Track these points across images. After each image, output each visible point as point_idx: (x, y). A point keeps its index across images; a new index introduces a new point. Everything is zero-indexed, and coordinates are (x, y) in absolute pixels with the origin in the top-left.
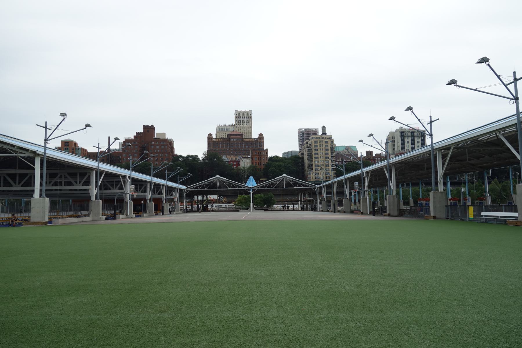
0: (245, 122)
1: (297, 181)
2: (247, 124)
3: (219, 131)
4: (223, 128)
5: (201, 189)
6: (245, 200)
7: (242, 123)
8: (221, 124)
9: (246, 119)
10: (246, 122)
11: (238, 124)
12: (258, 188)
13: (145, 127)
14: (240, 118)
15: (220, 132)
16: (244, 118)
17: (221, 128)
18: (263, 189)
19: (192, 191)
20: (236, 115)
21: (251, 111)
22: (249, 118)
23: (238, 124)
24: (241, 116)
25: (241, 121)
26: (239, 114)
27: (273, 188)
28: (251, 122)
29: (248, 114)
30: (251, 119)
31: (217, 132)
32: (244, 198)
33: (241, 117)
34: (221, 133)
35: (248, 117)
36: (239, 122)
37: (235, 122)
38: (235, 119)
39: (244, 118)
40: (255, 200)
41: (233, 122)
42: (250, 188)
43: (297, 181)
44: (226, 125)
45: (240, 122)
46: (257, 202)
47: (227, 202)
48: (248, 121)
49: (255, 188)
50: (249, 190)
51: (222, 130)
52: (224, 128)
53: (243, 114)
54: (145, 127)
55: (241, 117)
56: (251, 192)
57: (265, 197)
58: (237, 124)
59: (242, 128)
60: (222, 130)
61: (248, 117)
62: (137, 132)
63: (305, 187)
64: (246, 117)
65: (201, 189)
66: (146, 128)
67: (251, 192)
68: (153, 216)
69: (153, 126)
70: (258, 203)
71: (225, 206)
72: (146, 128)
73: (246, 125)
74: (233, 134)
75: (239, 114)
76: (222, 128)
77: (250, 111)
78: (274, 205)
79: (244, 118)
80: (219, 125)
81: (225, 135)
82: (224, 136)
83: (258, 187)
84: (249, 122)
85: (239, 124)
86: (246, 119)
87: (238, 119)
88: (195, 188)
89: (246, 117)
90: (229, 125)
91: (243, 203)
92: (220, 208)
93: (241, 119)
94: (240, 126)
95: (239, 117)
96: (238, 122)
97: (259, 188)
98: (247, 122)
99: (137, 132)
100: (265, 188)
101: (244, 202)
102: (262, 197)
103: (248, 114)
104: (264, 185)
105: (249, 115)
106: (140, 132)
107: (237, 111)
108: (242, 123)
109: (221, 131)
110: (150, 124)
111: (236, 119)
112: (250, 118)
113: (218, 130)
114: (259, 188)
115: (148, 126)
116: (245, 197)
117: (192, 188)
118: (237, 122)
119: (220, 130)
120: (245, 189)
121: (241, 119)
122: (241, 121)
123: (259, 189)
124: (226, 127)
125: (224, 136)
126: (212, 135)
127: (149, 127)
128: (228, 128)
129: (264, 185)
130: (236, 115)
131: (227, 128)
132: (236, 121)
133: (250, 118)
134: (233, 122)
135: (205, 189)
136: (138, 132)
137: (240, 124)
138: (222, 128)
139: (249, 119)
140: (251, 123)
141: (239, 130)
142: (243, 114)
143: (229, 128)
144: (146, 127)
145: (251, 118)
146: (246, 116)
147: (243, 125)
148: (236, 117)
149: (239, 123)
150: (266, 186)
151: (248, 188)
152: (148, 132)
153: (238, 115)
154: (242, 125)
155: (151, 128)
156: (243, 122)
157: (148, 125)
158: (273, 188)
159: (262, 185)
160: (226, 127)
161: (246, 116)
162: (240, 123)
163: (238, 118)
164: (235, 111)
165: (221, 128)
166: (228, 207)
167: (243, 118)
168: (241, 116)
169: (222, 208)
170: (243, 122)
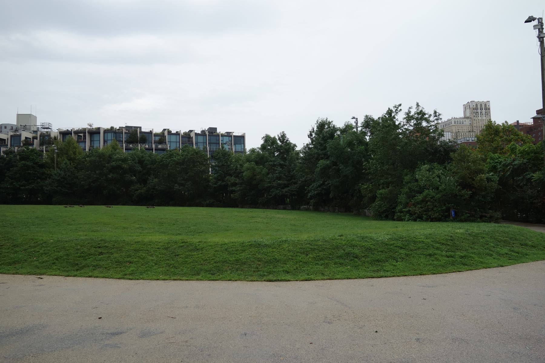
0: (483, 115)
3: (455, 124)
7: (479, 115)
9: (484, 111)
11: (476, 117)
14: (478, 109)
15: (456, 125)
16: (482, 109)
17: (456, 120)
20: (474, 106)
22: (487, 109)
23: (476, 117)
24: (479, 107)
26: (477, 105)
29: (485, 105)
33: (479, 109)
35: (486, 109)
36: (477, 114)
39: (481, 109)
48: (486, 113)
52: (460, 121)
53: (481, 105)
55: (479, 109)
58: (474, 117)
61: (486, 109)
64: (484, 109)
73: (484, 118)
75: (477, 105)
76: (458, 121)
79: (481, 109)
81: (461, 129)
82: (460, 129)
85: (477, 116)
86: (484, 111)
93: (479, 111)
96: (476, 114)
103: (485, 105)
105: (487, 107)
107: (474, 101)
108: (479, 115)
111: (474, 110)
112: (488, 109)
121: (479, 111)
125: (460, 129)
130: (474, 106)
131: (463, 121)
133: (488, 109)
137: (478, 117)
138: (458, 121)
140: (490, 115)
141: (478, 123)
142: (481, 105)
145: (489, 109)
146: (483, 107)
147: (481, 118)
149: (477, 115)
154: (480, 118)
156: (481, 115)
161: (483, 107)
163: (476, 109)
165: (456, 120)
167: (480, 109)
168: (479, 107)
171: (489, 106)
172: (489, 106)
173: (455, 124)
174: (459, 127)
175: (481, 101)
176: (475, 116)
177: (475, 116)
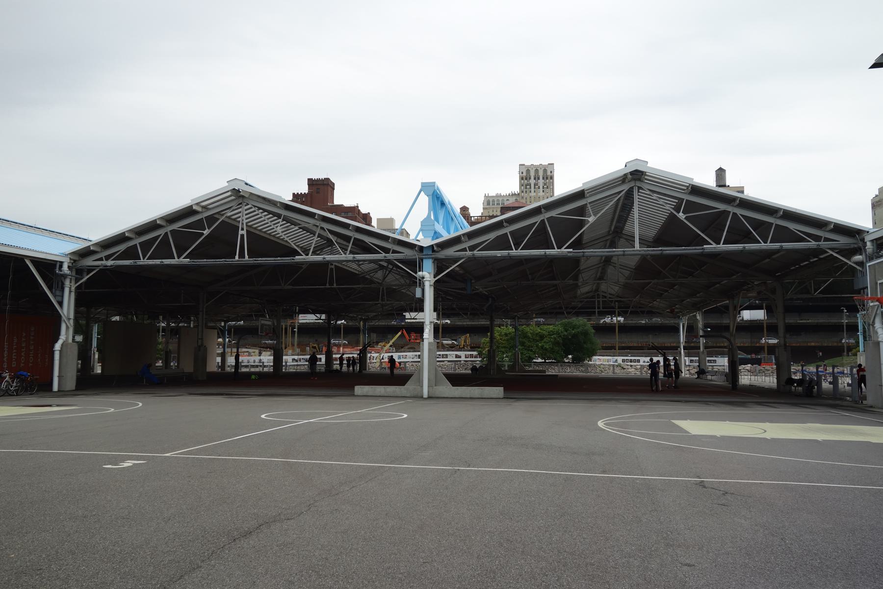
0: (539, 188)
1: (722, 207)
2: (543, 191)
3: (488, 207)
4: (496, 200)
5: (151, 262)
6: (507, 340)
8: (493, 193)
9: (541, 182)
10: (541, 187)
11: (526, 192)
12: (469, 253)
13: (311, 183)
14: (530, 178)
15: (490, 208)
16: (539, 179)
17: (491, 200)
18: (503, 259)
19: (104, 271)
20: (522, 173)
21: (553, 164)
22: (547, 178)
23: (526, 192)
24: (532, 174)
25: (532, 186)
26: (528, 171)
27: (564, 250)
28: (551, 187)
29: (545, 171)
30: (551, 181)
31: (484, 208)
32: (506, 335)
33: (532, 178)
34: (492, 210)
35: (546, 178)
37: (520, 188)
38: (520, 182)
39: (537, 178)
40: (537, 341)
41: (516, 189)
42: (421, 249)
43: (722, 207)
44: (502, 195)
45: (530, 188)
46: (542, 347)
47: (471, 348)
48: (545, 184)
49: (450, 252)
50: (415, 265)
51: (492, 205)
52: (498, 200)
53: (537, 171)
54: (311, 183)
55: (532, 178)
56: (427, 274)
57: (566, 333)
58: (522, 192)
59: (533, 198)
60: (494, 205)
61: (546, 178)
62: (294, 194)
63: (776, 246)
64: (541, 178)
65: (151, 262)
66: (313, 185)
67: (427, 274)
68: (14, 395)
69: (328, 179)
70: (546, 349)
71: (457, 356)
72: (313, 185)
74: (512, 207)
75: (528, 171)
76: (493, 201)
77: (549, 164)
78: (595, 358)
79: (537, 178)
80: (487, 195)
83: (472, 248)
84: (547, 188)
86: (541, 182)
87: (526, 181)
88: (124, 255)
89: (541, 178)
90: (508, 195)
91: (503, 350)
92: (444, 361)
93: (532, 181)
94: (531, 194)
95: (528, 178)
96: (526, 188)
97: (476, 253)
98: (543, 187)
99: (294, 194)
100: (514, 252)
101: (504, 347)
102: (558, 333)
103: (545, 171)
104: (507, 230)
105: (549, 173)
106: (298, 193)
107: (524, 165)
109: (491, 206)
110: (322, 176)
111: (522, 181)
112: (549, 178)
113: (486, 204)
114: (476, 253)
115: (318, 180)
116: (510, 334)
117: (108, 258)
118: (522, 187)
119: (488, 204)
120: (390, 256)
121: (532, 181)
122: (532, 186)
123: (473, 259)
124: (500, 199)
126: (468, 209)
127: (320, 183)
128: (505, 199)
129: (507, 230)
130: (522, 173)
132: (521, 185)
133: (549, 178)
134: (516, 189)
135: (175, 261)
136: (298, 193)
137: (530, 192)
138: (493, 201)
139: (547, 181)
142: (537, 171)
143: (508, 200)
144: (314, 183)
145: (552, 178)
146: (541, 174)
147: (535, 194)
148: (522, 178)
150: (518, 237)
151: (407, 253)
152: (318, 193)
153: (525, 174)
154: (533, 194)
155: (325, 184)
156: (535, 188)
157: (318, 178)
158: (564, 250)
159: (492, 236)
160: (500, 199)
161: (541, 174)
162: (529, 190)
163: (526, 179)
164: (520, 165)
165: (491, 200)
166: (463, 358)
167: (535, 179)
168: (532, 174)
169: (449, 361)
170: (537, 187)
171: (551, 172)
172: (551, 172)
173: (488, 207)
174: (495, 210)
175: (536, 163)
176: (525, 192)
177: (525, 192)
